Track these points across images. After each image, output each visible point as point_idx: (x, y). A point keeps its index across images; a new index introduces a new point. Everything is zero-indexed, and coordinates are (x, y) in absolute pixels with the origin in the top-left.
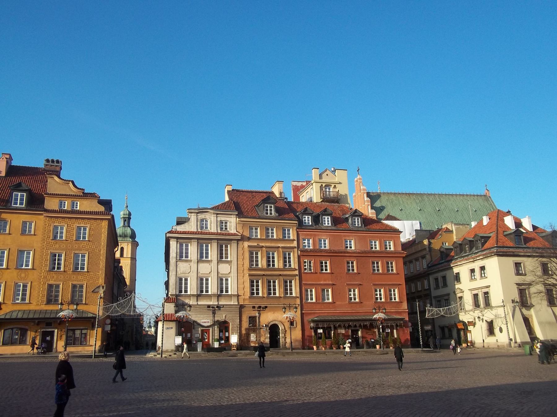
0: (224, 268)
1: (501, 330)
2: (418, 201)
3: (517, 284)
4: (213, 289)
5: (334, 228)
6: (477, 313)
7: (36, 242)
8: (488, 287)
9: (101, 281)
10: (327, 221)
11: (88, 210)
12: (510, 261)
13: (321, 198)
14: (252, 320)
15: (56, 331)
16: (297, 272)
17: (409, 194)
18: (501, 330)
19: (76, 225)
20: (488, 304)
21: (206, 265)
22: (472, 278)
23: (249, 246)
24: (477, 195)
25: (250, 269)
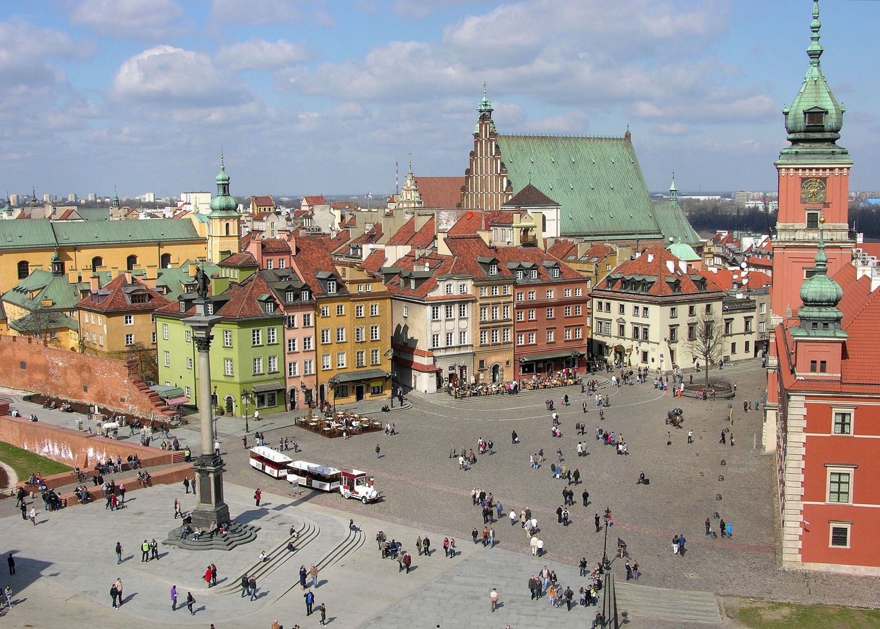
0: (463, 324)
1: (653, 360)
2: (551, 149)
3: (671, 326)
4: (455, 342)
6: (635, 344)
7: (346, 322)
8: (648, 325)
9: (389, 346)
10: (535, 274)
12: (668, 309)
14: (482, 362)
15: (364, 386)
16: (512, 322)
17: (542, 138)
18: (653, 360)
20: (646, 338)
22: (636, 315)
24: (617, 139)
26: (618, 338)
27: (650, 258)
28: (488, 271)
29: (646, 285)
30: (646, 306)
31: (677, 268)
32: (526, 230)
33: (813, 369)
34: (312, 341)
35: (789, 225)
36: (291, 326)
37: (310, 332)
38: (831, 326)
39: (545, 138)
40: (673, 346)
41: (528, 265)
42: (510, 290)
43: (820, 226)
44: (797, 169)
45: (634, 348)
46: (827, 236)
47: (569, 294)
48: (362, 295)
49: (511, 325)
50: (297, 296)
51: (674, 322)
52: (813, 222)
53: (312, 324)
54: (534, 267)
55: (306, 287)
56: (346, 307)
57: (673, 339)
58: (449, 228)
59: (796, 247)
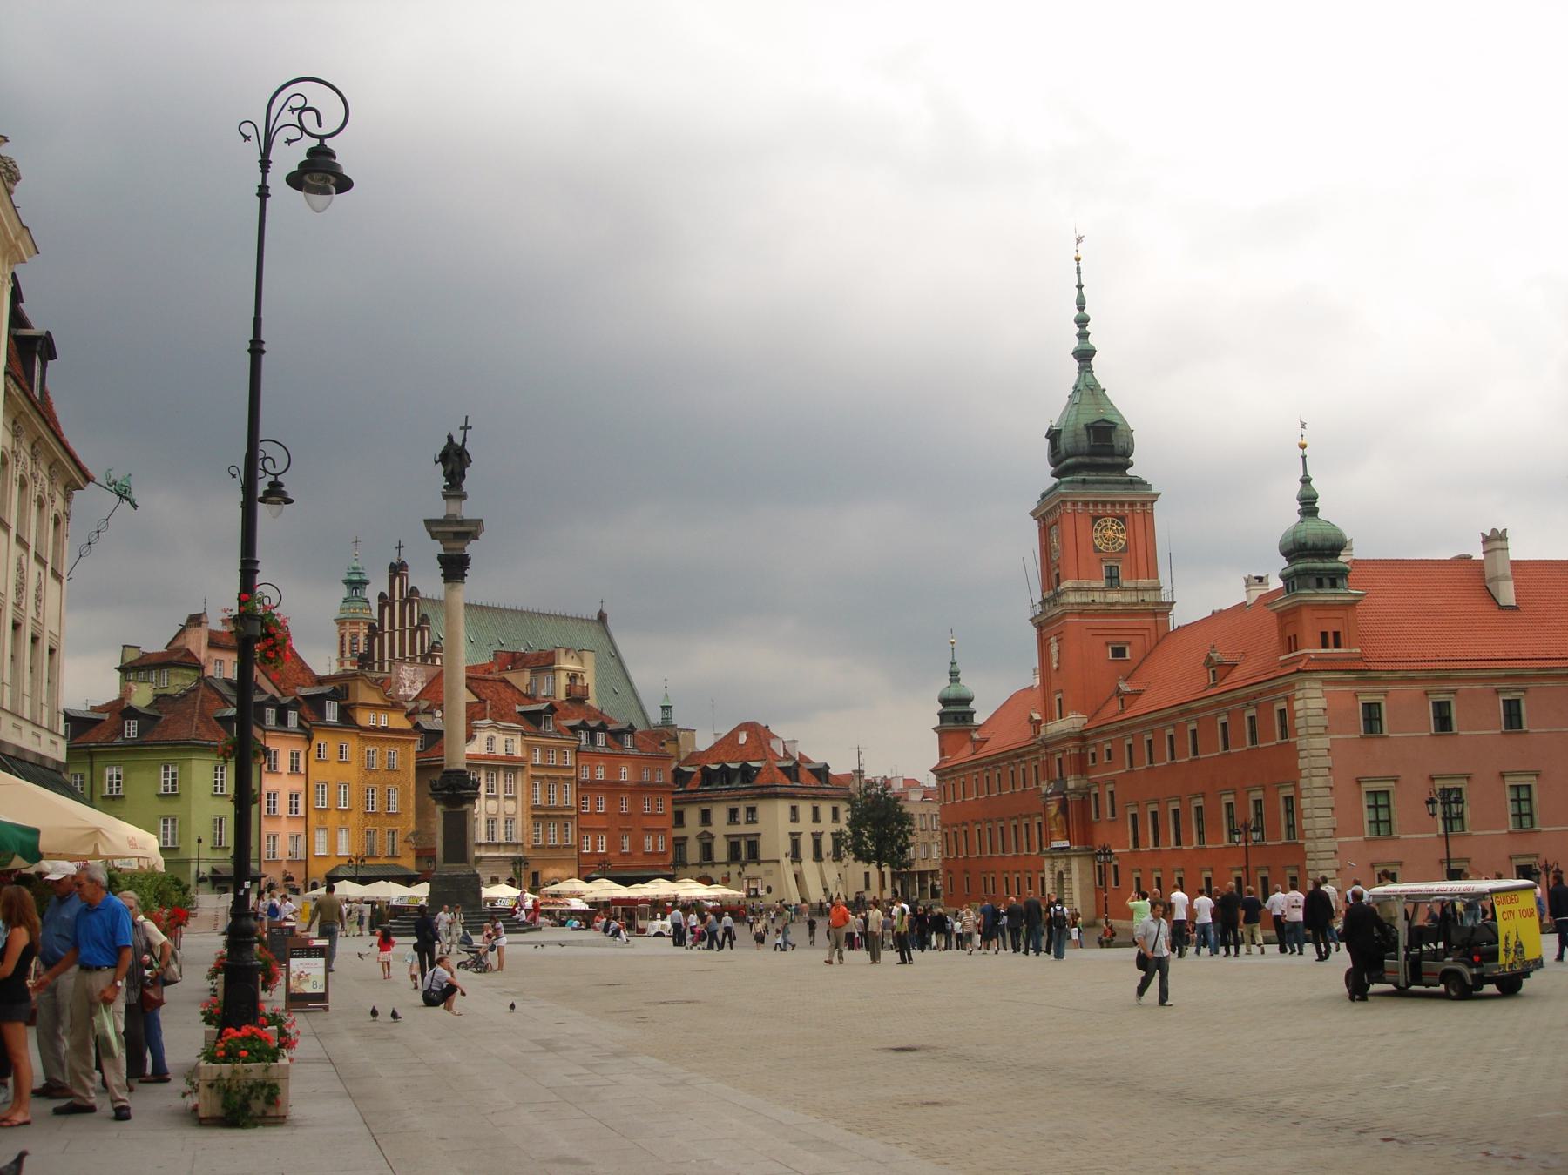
0: (510, 806)
3: (792, 834)
5: (608, 750)
6: (735, 869)
7: (352, 772)
8: (758, 835)
9: (412, 827)
11: (397, 726)
13: (568, 694)
17: (481, 607)
18: (769, 890)
19: (387, 749)
20: (754, 856)
21: (492, 803)
23: (533, 777)
25: (534, 808)
26: (700, 865)
27: (743, 738)
28: (539, 725)
29: (747, 773)
30: (751, 803)
31: (785, 752)
32: (573, 677)
33: (1325, 646)
34: (302, 801)
35: (1084, 583)
36: (273, 769)
37: (298, 784)
38: (1339, 582)
39: (487, 608)
40: (796, 865)
41: (593, 724)
42: (570, 759)
43: (1125, 583)
44: (1086, 504)
45: (734, 876)
46: (1131, 598)
47: (647, 777)
48: (375, 729)
49: (571, 817)
50: (282, 720)
51: (795, 828)
52: (1113, 580)
53: (302, 769)
54: (602, 727)
55: (295, 704)
56: (353, 745)
57: (796, 856)
58: (415, 693)
59: (1096, 614)
